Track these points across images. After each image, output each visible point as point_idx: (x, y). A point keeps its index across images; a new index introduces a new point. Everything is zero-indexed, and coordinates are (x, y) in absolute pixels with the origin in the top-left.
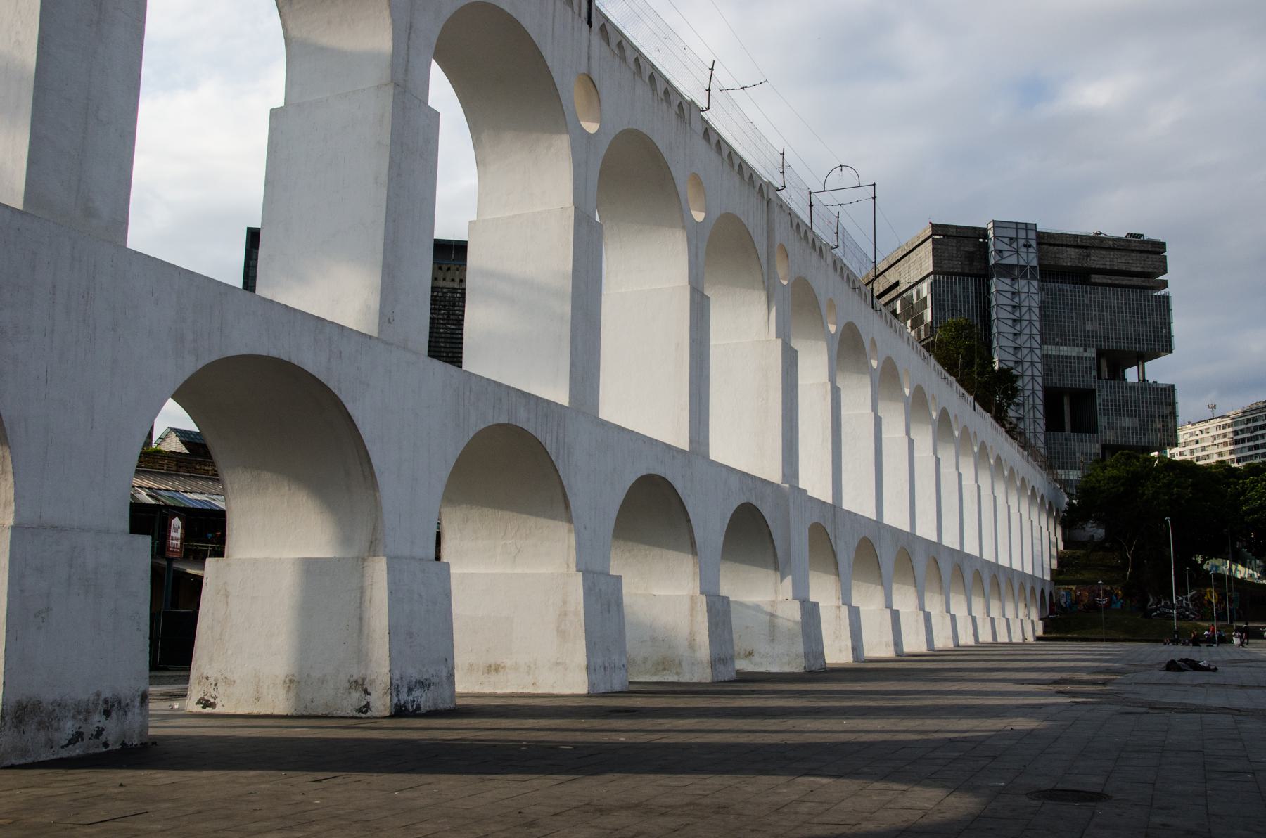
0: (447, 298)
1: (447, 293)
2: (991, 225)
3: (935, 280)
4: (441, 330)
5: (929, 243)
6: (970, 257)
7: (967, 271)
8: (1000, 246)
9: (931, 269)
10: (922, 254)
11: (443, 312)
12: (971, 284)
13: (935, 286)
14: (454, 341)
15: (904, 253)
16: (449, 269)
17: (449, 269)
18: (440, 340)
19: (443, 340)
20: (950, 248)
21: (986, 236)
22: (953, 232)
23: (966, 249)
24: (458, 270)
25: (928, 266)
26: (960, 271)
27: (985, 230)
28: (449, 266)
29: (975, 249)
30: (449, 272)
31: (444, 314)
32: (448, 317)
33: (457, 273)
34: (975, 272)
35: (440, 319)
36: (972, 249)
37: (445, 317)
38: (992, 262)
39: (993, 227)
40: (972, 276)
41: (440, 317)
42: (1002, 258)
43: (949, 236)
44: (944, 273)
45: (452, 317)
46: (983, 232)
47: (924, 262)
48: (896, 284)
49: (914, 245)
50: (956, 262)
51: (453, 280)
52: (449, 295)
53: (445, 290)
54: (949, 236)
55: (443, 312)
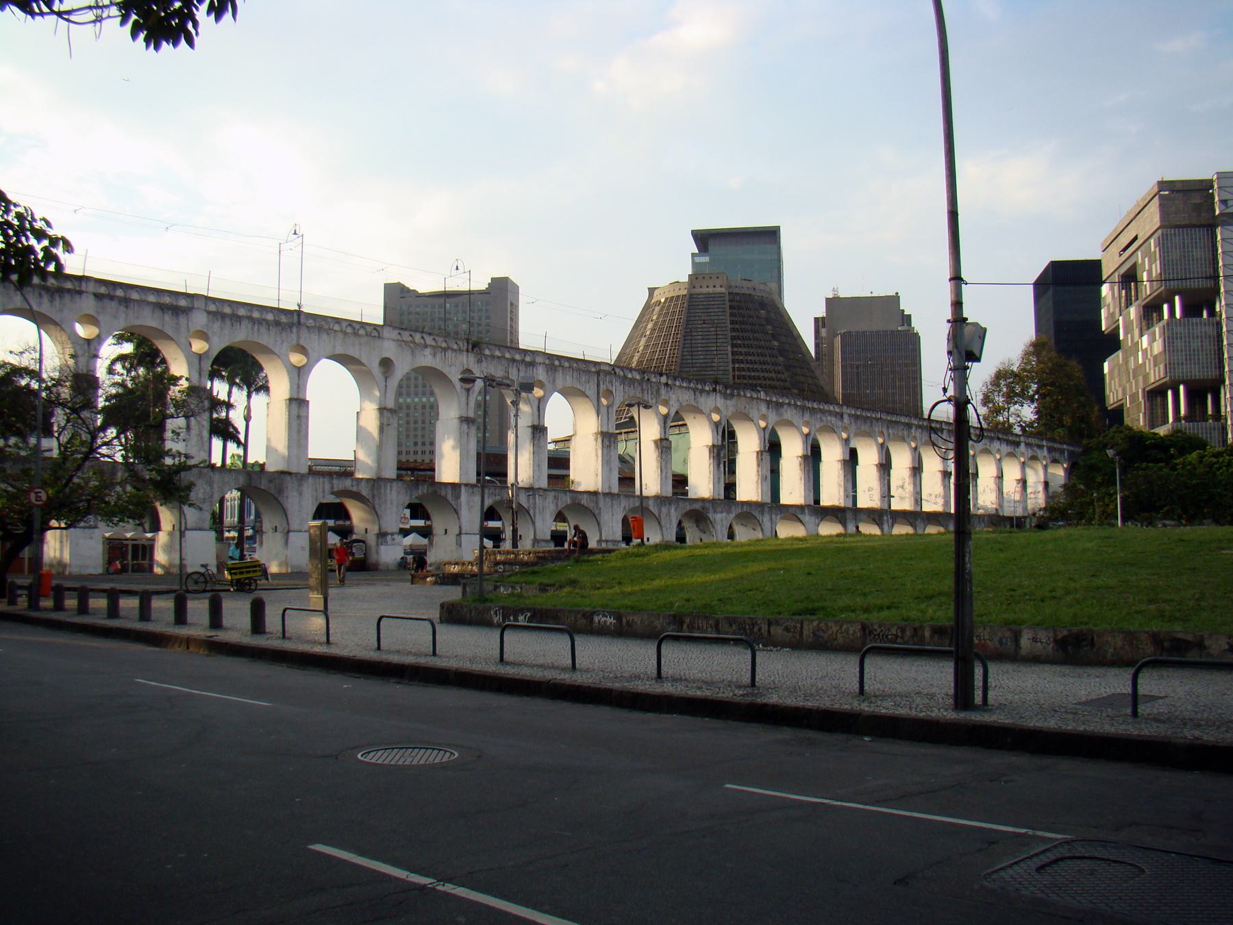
2: (1215, 177)
3: (1163, 235)
5: (1156, 201)
6: (1197, 208)
7: (1194, 222)
8: (1226, 196)
9: (1158, 225)
10: (1152, 210)
12: (1200, 234)
13: (1163, 240)
15: (1140, 208)
20: (1176, 202)
21: (1212, 187)
22: (1179, 187)
23: (1194, 201)
25: (1156, 221)
26: (1187, 223)
27: (1211, 181)
29: (1202, 201)
34: (1203, 222)
36: (1198, 201)
38: (1217, 212)
39: (1218, 178)
40: (1199, 226)
42: (1227, 207)
43: (1178, 191)
44: (1171, 227)
46: (1208, 184)
47: (1152, 219)
48: (1136, 238)
49: (1147, 201)
50: (1183, 215)
51: (708, 287)
54: (1178, 191)
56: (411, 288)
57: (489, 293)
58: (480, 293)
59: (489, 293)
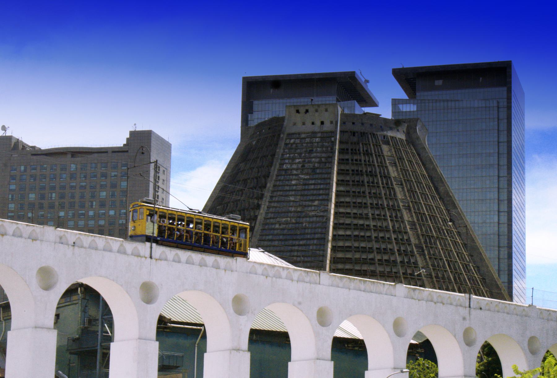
0: (304, 145)
1: (305, 138)
4: (293, 182)
11: (297, 161)
14: (306, 193)
16: (307, 111)
17: (307, 111)
18: (291, 193)
19: (293, 193)
24: (317, 111)
28: (307, 108)
30: (307, 113)
31: (299, 163)
32: (303, 166)
33: (317, 114)
35: (294, 169)
37: (300, 166)
41: (295, 166)
45: (306, 165)
52: (308, 140)
53: (303, 136)
55: (297, 161)
56: (31, 145)
57: (127, 151)
58: (115, 151)
59: (127, 151)
